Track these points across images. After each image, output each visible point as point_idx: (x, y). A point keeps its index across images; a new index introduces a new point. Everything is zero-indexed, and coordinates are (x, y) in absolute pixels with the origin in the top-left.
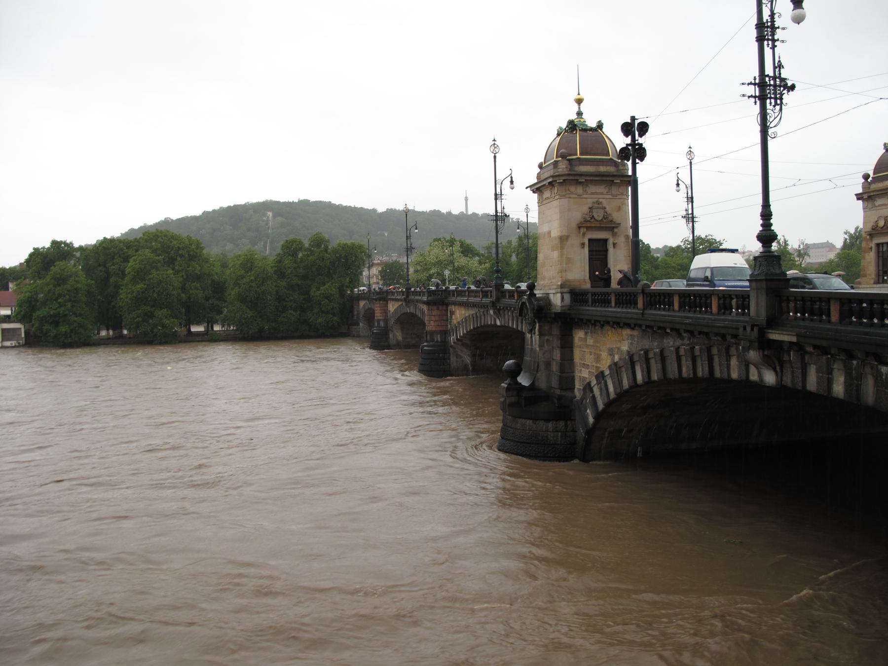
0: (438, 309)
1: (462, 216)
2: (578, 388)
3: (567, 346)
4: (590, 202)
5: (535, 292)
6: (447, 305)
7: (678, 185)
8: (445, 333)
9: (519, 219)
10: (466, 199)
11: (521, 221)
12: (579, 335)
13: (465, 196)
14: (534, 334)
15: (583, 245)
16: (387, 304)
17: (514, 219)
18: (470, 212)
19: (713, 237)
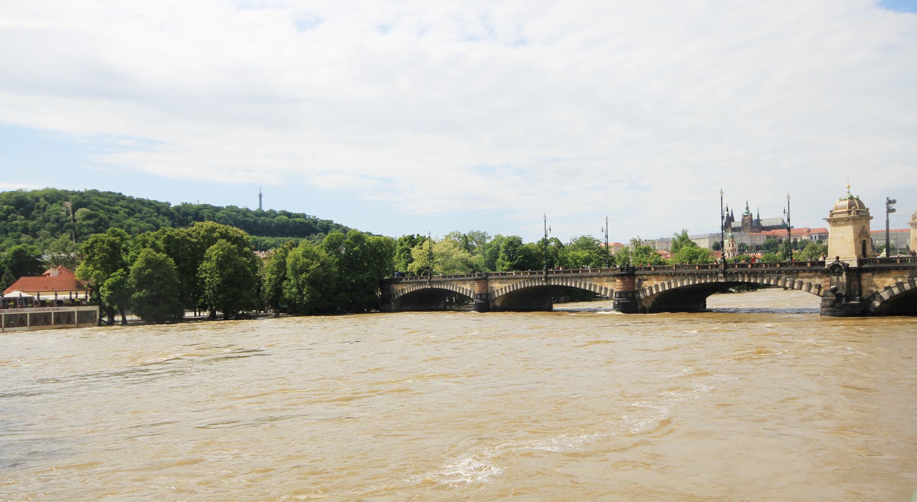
0: (629, 278)
1: (260, 214)
2: (865, 295)
3: (859, 280)
4: (861, 226)
5: (839, 260)
6: (635, 276)
7: (784, 213)
8: (635, 293)
9: (315, 217)
10: (260, 196)
11: (318, 219)
12: (866, 276)
13: (259, 193)
14: (841, 276)
15: (861, 242)
16: (488, 282)
17: (311, 217)
18: (266, 209)
19: (592, 237)
